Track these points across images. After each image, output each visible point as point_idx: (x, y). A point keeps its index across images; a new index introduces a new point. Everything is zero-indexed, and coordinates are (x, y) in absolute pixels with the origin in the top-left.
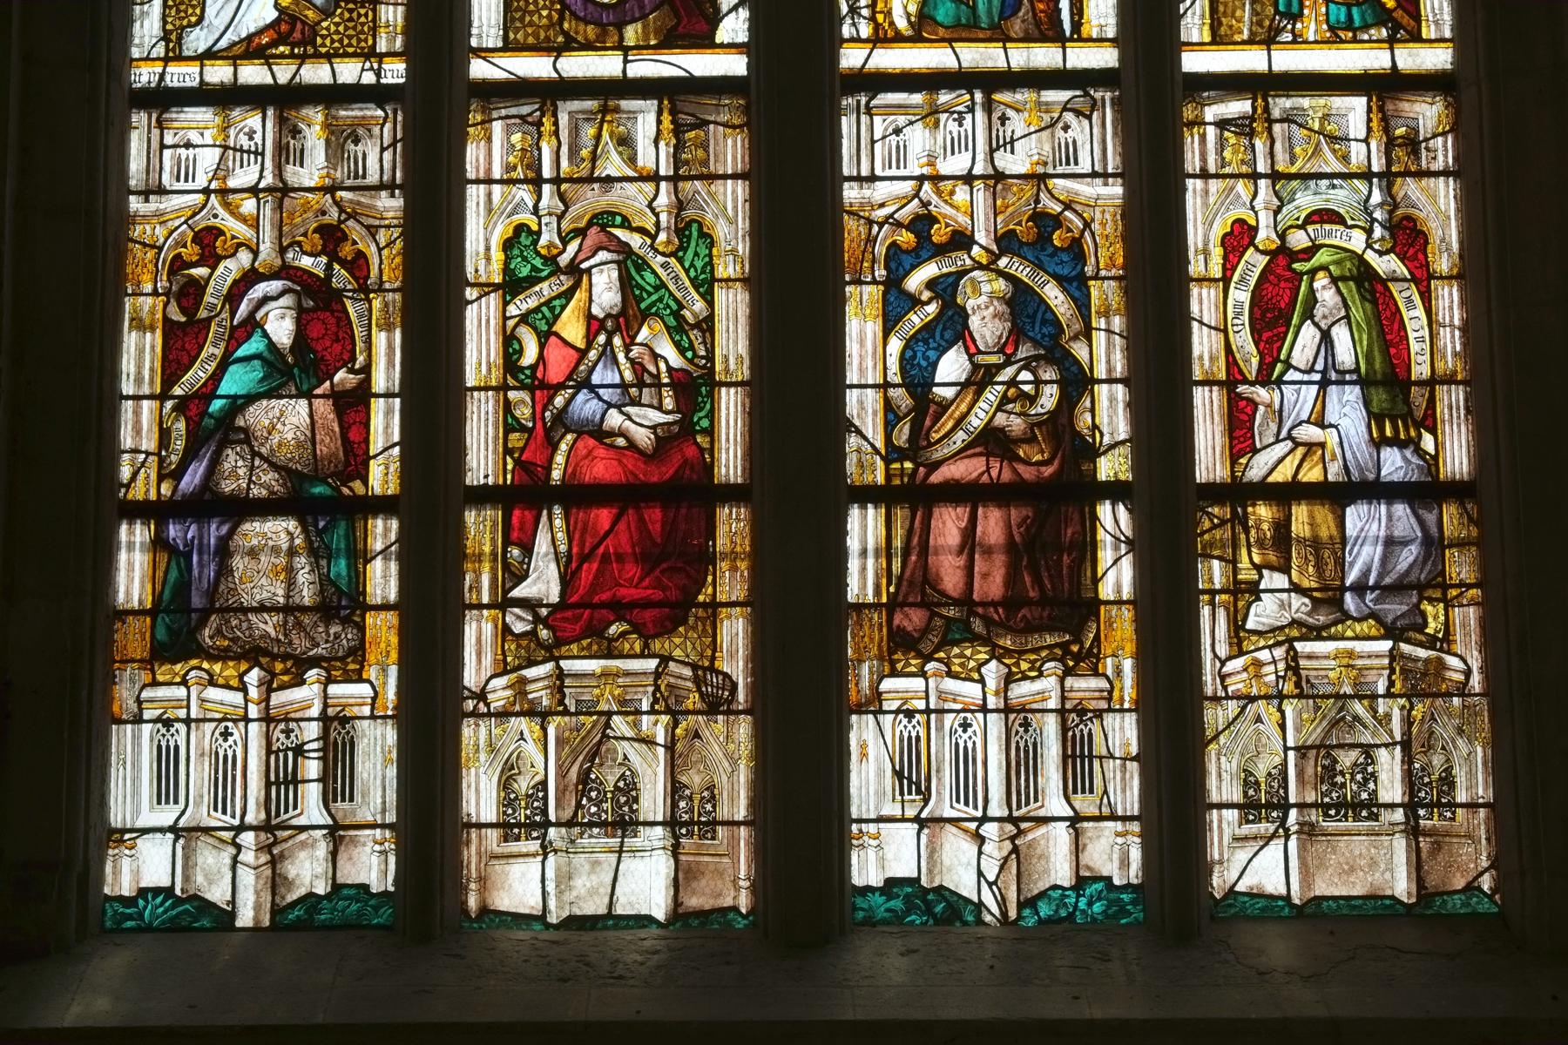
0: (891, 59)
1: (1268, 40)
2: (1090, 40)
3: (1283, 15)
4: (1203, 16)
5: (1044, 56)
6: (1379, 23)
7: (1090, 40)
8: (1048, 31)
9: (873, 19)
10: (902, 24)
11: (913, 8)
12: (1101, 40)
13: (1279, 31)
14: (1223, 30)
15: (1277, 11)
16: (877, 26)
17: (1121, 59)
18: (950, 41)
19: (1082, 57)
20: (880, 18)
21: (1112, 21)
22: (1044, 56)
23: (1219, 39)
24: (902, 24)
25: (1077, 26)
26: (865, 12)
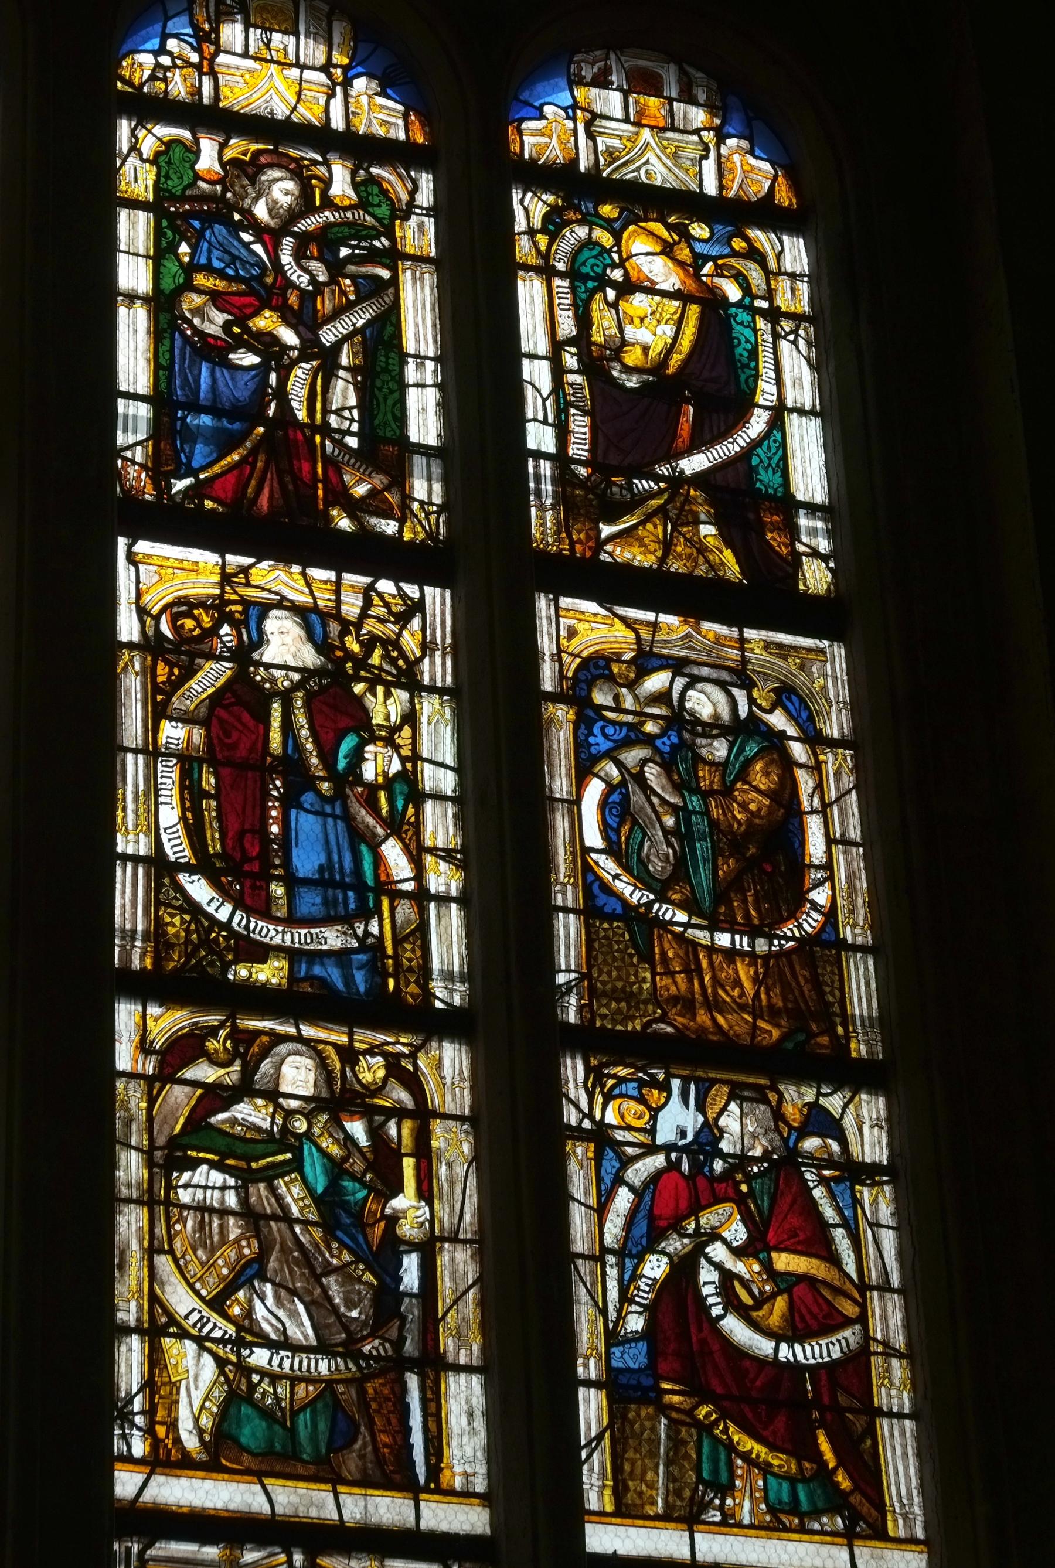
0: (177, 1491)
1: (689, 1518)
2: (452, 1492)
3: (709, 1485)
4: (603, 1475)
5: (388, 1509)
6: (833, 1510)
7: (452, 1492)
8: (394, 1474)
9: (149, 1431)
10: (191, 1442)
11: (206, 1422)
12: (466, 1495)
13: (706, 1506)
14: (630, 1497)
15: (700, 1479)
16: (156, 1443)
17: (492, 1524)
18: (259, 1475)
19: (443, 1517)
20: (161, 1431)
21: (482, 1469)
22: (388, 1509)
23: (626, 1510)
24: (191, 1442)
25: (434, 1470)
26: (139, 1420)
